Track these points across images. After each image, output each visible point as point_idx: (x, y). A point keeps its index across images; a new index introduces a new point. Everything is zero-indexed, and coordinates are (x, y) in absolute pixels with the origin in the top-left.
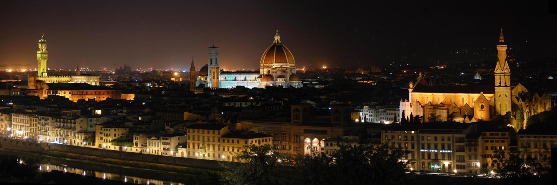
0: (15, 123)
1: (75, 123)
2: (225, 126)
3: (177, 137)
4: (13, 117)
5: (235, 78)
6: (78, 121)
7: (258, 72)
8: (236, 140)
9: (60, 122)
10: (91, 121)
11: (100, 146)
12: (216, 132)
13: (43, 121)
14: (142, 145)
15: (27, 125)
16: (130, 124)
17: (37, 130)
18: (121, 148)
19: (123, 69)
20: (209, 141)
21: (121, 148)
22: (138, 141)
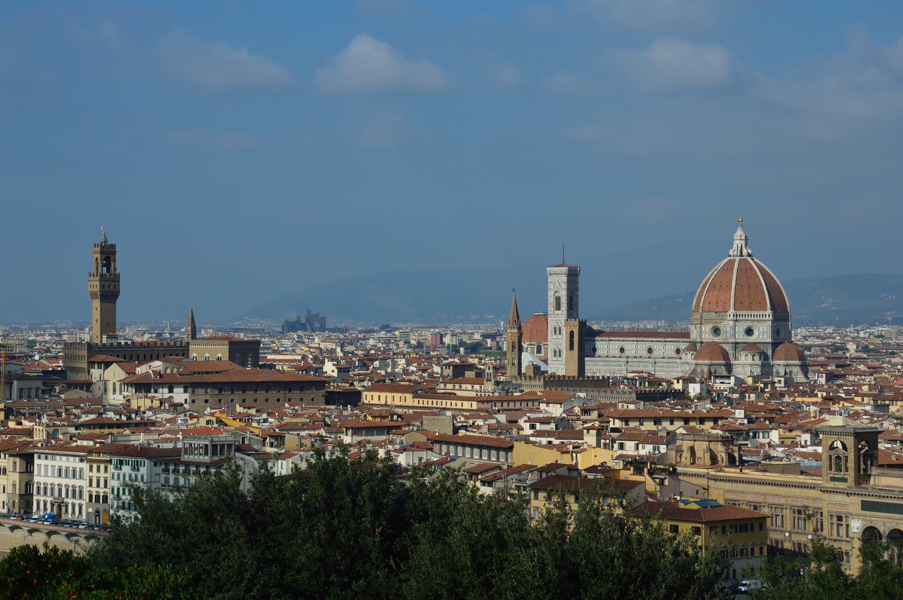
4: (37, 461)
5: (622, 350)
7: (687, 335)
15: (77, 483)
17: (111, 497)
19: (303, 321)
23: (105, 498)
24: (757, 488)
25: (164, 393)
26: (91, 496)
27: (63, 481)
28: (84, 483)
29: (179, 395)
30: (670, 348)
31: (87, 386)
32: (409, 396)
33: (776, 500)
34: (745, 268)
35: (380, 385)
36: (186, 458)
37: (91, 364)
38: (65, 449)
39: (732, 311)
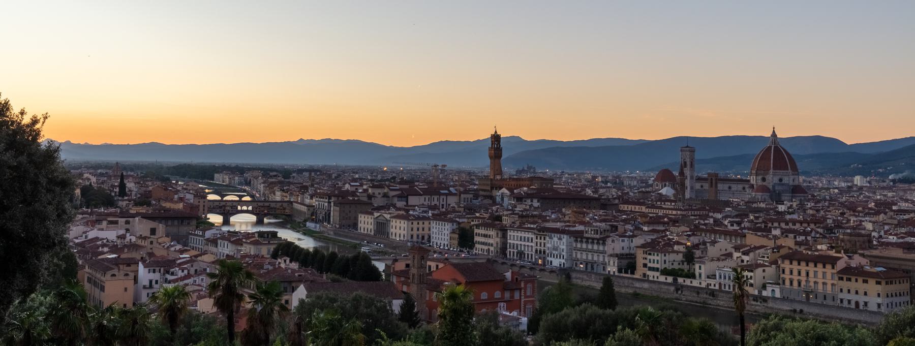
0: (512, 242)
1: (604, 244)
2: (840, 258)
3: (761, 269)
4: (509, 233)
6: (609, 241)
8: (860, 280)
9: (581, 242)
10: (623, 241)
11: (644, 275)
12: (829, 266)
13: (555, 239)
14: (708, 277)
15: (530, 244)
16: (681, 248)
17: (547, 252)
18: (675, 280)
20: (815, 276)
21: (675, 280)
22: (703, 271)
23: (544, 252)
24: (895, 262)
25: (529, 202)
26: (536, 250)
27: (523, 243)
28: (533, 244)
29: (536, 204)
30: (740, 187)
31: (492, 198)
32: (644, 208)
33: (907, 268)
34: (777, 150)
35: (627, 202)
36: (586, 235)
37: (492, 188)
38: (521, 228)
39: (771, 171)
